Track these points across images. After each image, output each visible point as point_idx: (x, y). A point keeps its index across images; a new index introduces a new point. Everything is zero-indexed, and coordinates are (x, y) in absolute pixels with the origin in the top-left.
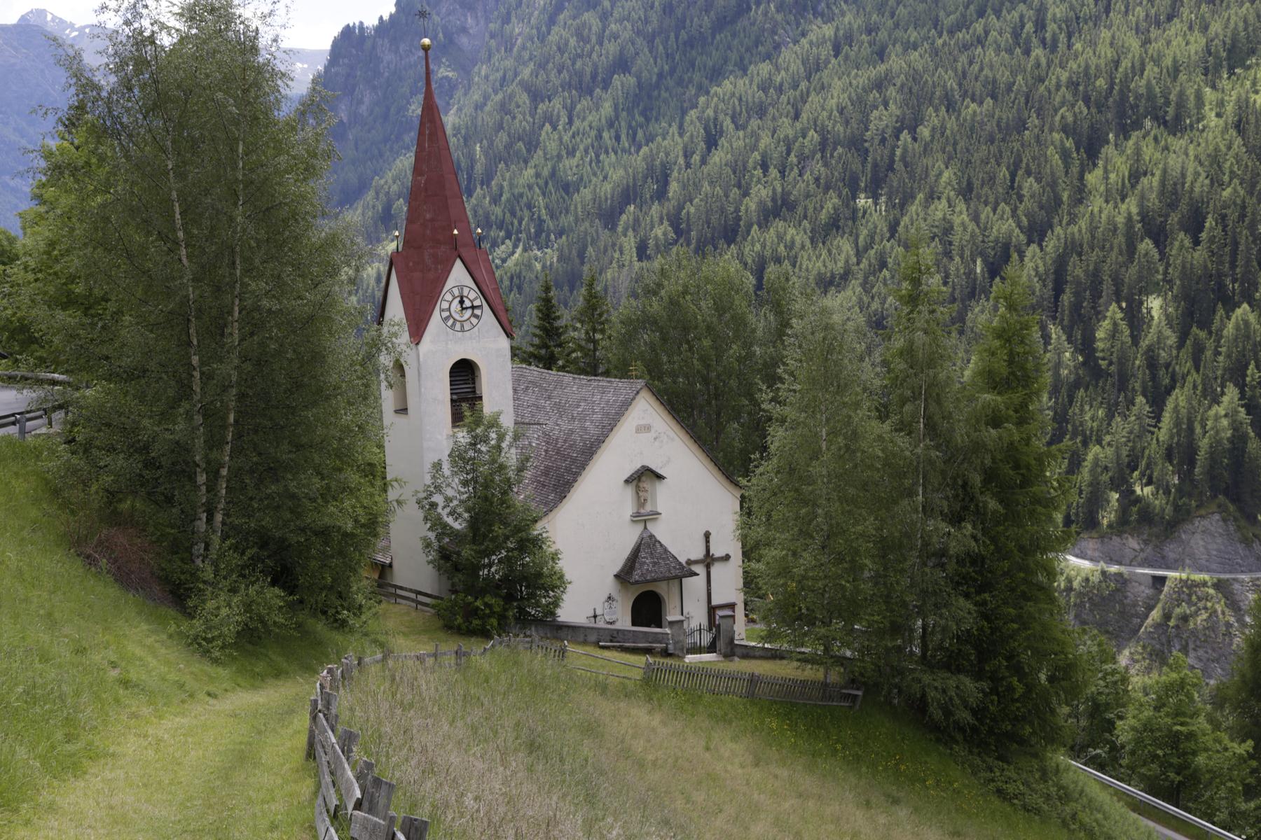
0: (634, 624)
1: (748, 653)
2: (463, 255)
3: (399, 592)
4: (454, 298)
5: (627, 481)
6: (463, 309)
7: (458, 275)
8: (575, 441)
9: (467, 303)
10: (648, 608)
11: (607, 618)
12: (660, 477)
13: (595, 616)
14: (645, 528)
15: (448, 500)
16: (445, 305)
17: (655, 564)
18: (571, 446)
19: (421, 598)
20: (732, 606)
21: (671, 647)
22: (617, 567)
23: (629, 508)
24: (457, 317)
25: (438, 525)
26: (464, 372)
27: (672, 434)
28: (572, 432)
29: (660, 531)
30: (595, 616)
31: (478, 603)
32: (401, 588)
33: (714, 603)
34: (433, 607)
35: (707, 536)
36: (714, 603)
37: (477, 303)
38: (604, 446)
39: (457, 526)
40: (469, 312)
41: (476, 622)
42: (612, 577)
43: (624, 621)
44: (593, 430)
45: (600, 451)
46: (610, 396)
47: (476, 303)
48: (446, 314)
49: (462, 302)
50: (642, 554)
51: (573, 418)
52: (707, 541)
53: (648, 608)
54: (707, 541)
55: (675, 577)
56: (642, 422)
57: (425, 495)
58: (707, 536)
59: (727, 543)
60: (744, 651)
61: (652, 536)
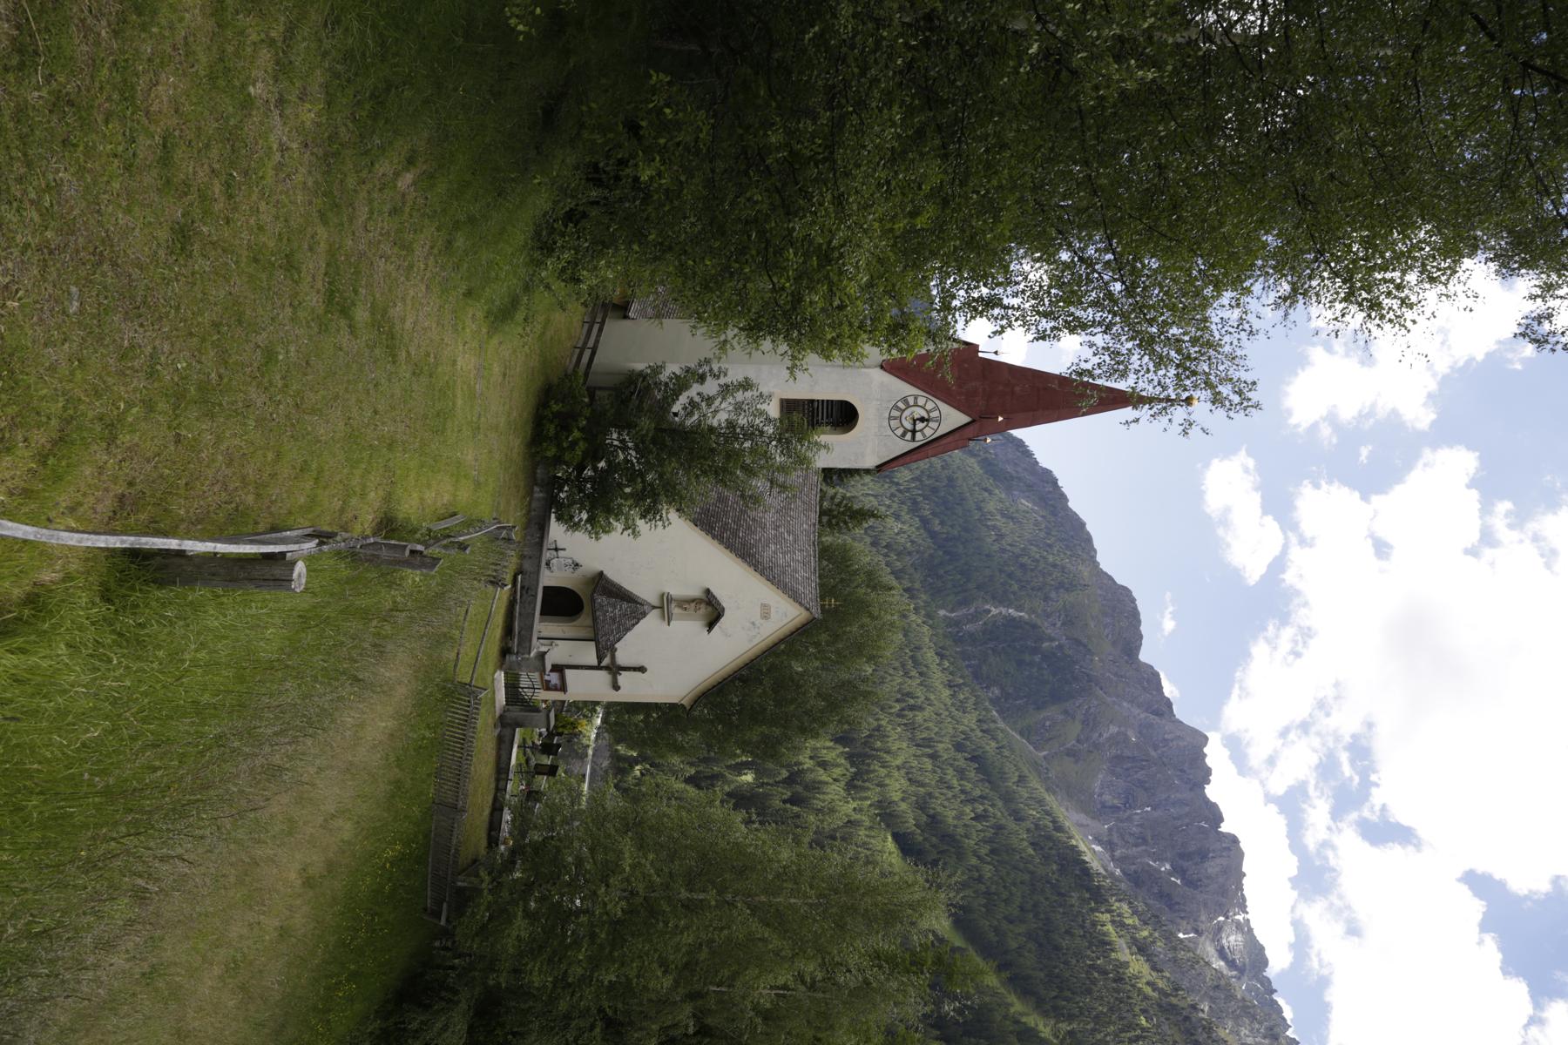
0: (545, 588)
1: (503, 744)
2: (971, 428)
3: (596, 327)
5: (708, 591)
6: (915, 421)
7: (953, 418)
8: (754, 533)
9: (920, 426)
10: (562, 604)
11: (554, 561)
12: (711, 625)
13: (556, 549)
15: (709, 400)
16: (921, 401)
17: (613, 619)
18: (749, 528)
19: (587, 353)
21: (514, 658)
22: (611, 574)
23: (677, 591)
24: (907, 413)
25: (681, 384)
26: (843, 416)
27: (756, 641)
28: (764, 527)
29: (651, 621)
30: (556, 549)
31: (576, 434)
32: (600, 330)
33: (568, 672)
34: (575, 371)
35: (642, 669)
36: (568, 672)
37: (919, 436)
38: (751, 570)
39: (676, 408)
40: (909, 426)
41: (552, 429)
42: (600, 568)
43: (548, 578)
44: (768, 553)
45: (745, 566)
46: (802, 574)
49: (922, 420)
50: (625, 605)
51: (777, 528)
53: (562, 604)
54: (635, 669)
55: (596, 634)
57: (716, 369)
58: (642, 669)
59: (633, 689)
60: (507, 739)
61: (644, 614)
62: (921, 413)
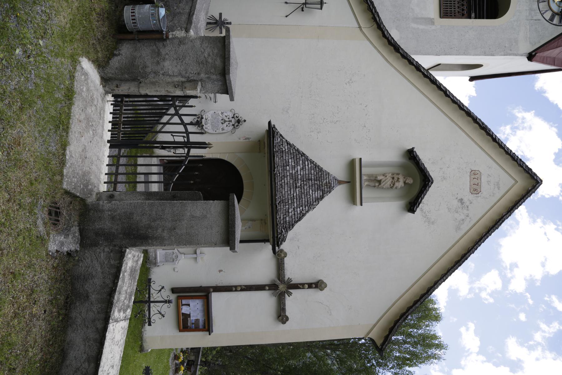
12: (412, 206)
20: (207, 327)
27: (465, 227)
35: (318, 285)
36: (216, 298)
52: (310, 286)
54: (310, 286)
56: (484, 179)
58: (318, 285)
61: (330, 188)
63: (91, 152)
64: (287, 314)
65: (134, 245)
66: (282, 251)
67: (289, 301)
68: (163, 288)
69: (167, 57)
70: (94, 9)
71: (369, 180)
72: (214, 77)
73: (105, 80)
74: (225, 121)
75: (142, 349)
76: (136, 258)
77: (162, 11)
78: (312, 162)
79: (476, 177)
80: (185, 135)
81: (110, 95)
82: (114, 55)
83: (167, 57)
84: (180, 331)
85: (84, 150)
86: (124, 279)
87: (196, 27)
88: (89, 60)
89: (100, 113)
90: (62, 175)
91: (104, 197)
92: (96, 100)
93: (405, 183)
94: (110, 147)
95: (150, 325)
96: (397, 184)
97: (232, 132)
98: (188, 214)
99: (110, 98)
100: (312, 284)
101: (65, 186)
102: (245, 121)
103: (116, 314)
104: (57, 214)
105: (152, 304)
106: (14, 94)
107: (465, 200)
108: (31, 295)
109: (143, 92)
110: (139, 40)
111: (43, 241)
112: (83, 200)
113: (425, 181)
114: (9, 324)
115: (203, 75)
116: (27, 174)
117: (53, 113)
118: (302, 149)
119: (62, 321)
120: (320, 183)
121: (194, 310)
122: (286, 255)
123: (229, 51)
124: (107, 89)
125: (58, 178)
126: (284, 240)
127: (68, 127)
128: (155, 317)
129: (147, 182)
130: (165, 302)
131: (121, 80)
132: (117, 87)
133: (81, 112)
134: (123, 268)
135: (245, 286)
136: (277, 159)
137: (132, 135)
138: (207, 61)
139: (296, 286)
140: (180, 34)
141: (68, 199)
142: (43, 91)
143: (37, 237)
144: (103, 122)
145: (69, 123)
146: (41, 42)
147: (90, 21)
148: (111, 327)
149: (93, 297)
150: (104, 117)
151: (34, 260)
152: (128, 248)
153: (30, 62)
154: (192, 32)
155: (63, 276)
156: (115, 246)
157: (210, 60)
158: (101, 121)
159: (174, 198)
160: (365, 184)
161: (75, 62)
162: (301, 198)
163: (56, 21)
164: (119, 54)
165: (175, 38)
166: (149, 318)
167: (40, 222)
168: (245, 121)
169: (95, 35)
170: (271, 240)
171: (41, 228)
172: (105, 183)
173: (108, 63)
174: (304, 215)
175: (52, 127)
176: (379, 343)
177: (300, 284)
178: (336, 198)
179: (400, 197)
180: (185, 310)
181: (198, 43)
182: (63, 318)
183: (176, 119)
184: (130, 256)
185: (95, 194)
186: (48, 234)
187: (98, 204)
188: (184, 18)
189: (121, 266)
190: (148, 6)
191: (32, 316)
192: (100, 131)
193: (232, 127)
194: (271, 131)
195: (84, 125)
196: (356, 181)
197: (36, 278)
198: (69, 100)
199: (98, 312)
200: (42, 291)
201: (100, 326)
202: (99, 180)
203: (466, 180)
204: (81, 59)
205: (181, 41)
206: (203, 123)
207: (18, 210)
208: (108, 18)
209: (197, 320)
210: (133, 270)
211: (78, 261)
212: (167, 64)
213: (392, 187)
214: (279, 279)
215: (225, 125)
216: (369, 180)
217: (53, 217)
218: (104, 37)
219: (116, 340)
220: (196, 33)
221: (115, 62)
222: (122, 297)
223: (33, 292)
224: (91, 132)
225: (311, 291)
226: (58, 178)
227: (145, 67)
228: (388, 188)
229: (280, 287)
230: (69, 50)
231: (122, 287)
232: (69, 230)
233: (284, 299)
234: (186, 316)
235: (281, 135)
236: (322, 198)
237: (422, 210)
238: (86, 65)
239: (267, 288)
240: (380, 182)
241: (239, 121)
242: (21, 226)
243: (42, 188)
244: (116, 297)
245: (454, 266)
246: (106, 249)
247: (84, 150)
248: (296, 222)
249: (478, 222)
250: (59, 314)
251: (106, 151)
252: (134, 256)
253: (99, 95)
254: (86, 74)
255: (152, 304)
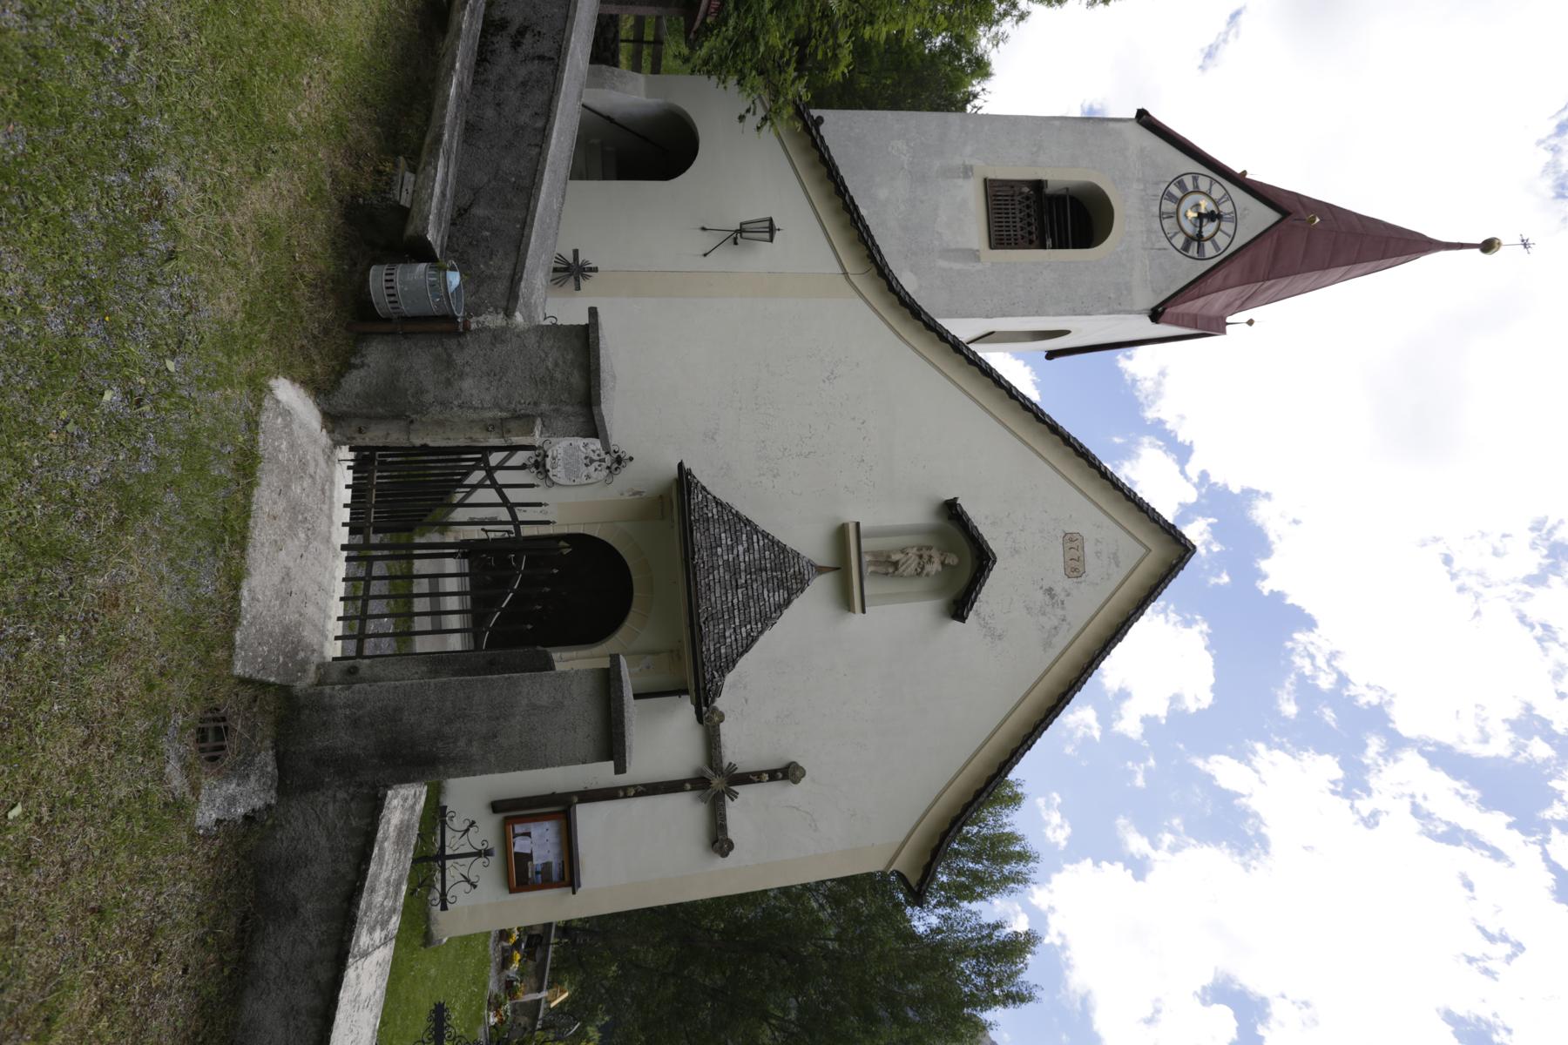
4: (1216, 203)
9: (1209, 228)
12: (959, 608)
14: (821, 570)
16: (1204, 184)
20: (567, 875)
27: (1060, 642)
35: (788, 773)
36: (587, 817)
37: (1209, 249)
47: (1208, 245)
48: (1188, 181)
49: (1213, 216)
52: (773, 775)
54: (773, 775)
56: (1089, 549)
58: (788, 773)
61: (802, 583)
62: (1205, 205)
63: (303, 574)
64: (731, 835)
65: (405, 780)
66: (715, 709)
67: (733, 810)
68: (472, 824)
69: (467, 369)
70: (302, 276)
71: (876, 563)
72: (569, 409)
73: (332, 419)
74: (592, 461)
75: (428, 939)
76: (410, 802)
77: (454, 279)
78: (766, 535)
79: (1074, 545)
80: (511, 528)
81: (345, 448)
82: (352, 367)
83: (467, 369)
84: (512, 891)
85: (287, 576)
86: (381, 856)
87: (527, 305)
88: (293, 380)
89: (323, 491)
90: (230, 645)
91: (335, 676)
92: (312, 464)
93: (942, 563)
94: (348, 559)
95: (444, 908)
96: (928, 568)
97: (607, 482)
98: (524, 702)
99: (345, 453)
100: (775, 771)
101: (239, 669)
102: (631, 459)
103: (363, 939)
104: (220, 733)
105: (449, 863)
106: (100, 493)
107: (1057, 589)
108: (147, 943)
109: (417, 442)
110: (406, 335)
111: (179, 808)
112: (284, 690)
113: (981, 559)
114: (83, 1033)
115: (544, 406)
116: (136, 669)
117: (204, 509)
118: (746, 511)
119: (230, 977)
120: (782, 574)
121: (540, 842)
122: (722, 717)
123: (598, 358)
124: (337, 436)
125: (220, 654)
126: (718, 693)
127: (244, 538)
128: (457, 891)
129: (435, 595)
130: (478, 854)
131: (369, 417)
132: (360, 431)
133: (275, 496)
134: (380, 835)
135: (644, 785)
136: (697, 536)
137: (399, 499)
138: (552, 378)
139: (747, 779)
140: (494, 320)
141: (247, 693)
142: (178, 469)
143: (166, 804)
144: (331, 508)
145: (246, 527)
146: (171, 365)
147: (292, 301)
148: (350, 974)
149: (309, 909)
150: (331, 497)
151: (158, 860)
152: (389, 787)
153: (143, 414)
154: (519, 317)
155: (234, 871)
156: (361, 785)
157: (558, 375)
158: (325, 507)
159: (491, 667)
160: (868, 570)
161: (258, 389)
162: (746, 606)
163: (207, 310)
164: (363, 365)
165: (483, 329)
166: (443, 894)
167: (173, 769)
168: (631, 459)
169: (305, 329)
170: (692, 688)
171: (177, 781)
172: (337, 638)
173: (336, 384)
174: (754, 640)
175: (201, 544)
176: (913, 880)
177: (754, 773)
178: (815, 598)
179: (935, 592)
180: (520, 845)
181: (532, 340)
182: (234, 970)
183: (490, 495)
184: (395, 802)
185: (313, 668)
186: (195, 789)
187: (321, 693)
188: (501, 287)
189: (376, 831)
190: (423, 266)
191: (149, 991)
192: (324, 528)
193: (605, 472)
194: (684, 480)
195: (284, 524)
196: (850, 566)
197: (161, 900)
198: (245, 476)
199: (321, 944)
200: (177, 925)
201: (324, 975)
202: (323, 634)
203: (1056, 556)
204: (273, 382)
205: (497, 336)
206: (548, 466)
207: (111, 757)
208: (333, 290)
209: (547, 865)
210: (403, 830)
211: (273, 827)
212: (467, 384)
213: (919, 574)
214: (711, 768)
215: (592, 468)
216: (876, 563)
217: (211, 742)
218: (326, 332)
219: (363, 997)
220: (529, 317)
221: (354, 382)
222: (378, 899)
223: (152, 935)
224: (302, 536)
225: (775, 786)
226: (220, 654)
227: (421, 391)
228: (911, 576)
229: (714, 782)
230: (243, 367)
231: (376, 876)
232: (251, 763)
233: (723, 806)
234: (523, 858)
235: (704, 488)
236: (788, 602)
237: (978, 614)
238: (287, 392)
239: (688, 786)
240: (896, 564)
241: (619, 460)
242: (122, 791)
243: (177, 690)
244: (363, 905)
245: (1046, 717)
246: (341, 795)
247: (287, 576)
248: (741, 655)
249: (1083, 629)
250: (222, 963)
251: (341, 569)
252: (405, 800)
253: (319, 451)
254: (287, 413)
255: (449, 863)
